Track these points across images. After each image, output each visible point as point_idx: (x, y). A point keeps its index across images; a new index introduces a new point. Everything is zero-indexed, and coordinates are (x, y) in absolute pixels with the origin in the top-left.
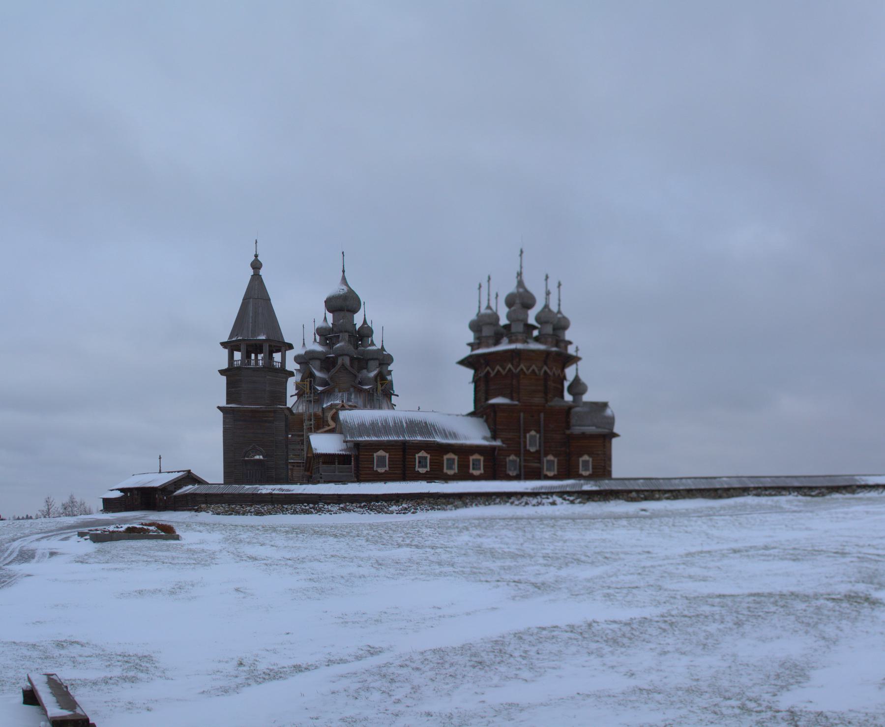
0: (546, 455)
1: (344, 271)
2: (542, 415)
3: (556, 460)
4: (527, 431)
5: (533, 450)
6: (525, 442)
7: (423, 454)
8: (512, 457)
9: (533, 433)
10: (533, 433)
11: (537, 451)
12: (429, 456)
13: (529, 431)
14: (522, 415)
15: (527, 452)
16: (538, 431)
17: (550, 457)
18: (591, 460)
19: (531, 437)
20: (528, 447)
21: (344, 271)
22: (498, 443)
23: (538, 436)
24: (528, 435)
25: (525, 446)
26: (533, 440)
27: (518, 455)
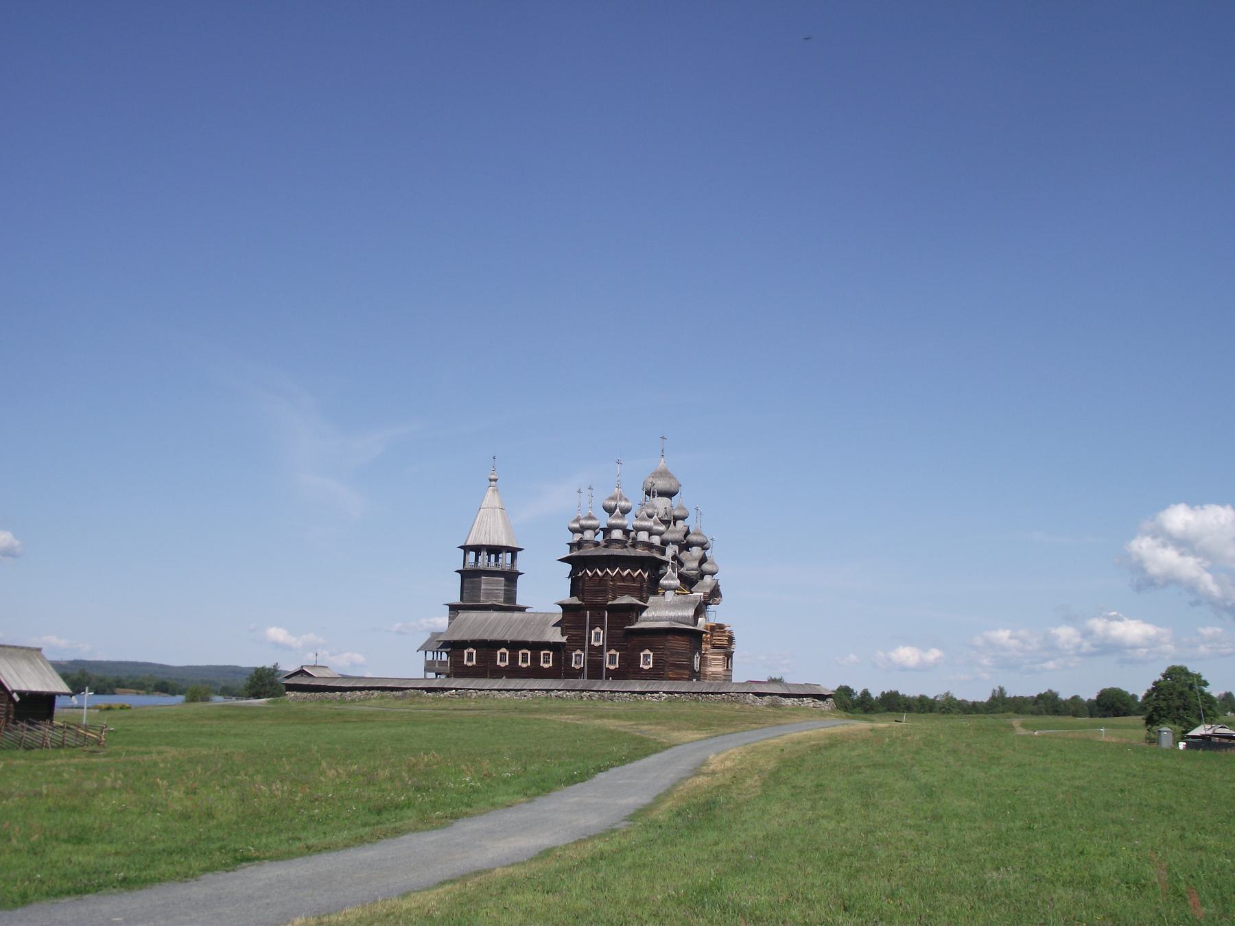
4: (591, 628)
5: (597, 644)
8: (578, 652)
9: (598, 629)
10: (598, 629)
15: (591, 647)
16: (602, 628)
17: (613, 652)
22: (564, 640)
27: (583, 650)
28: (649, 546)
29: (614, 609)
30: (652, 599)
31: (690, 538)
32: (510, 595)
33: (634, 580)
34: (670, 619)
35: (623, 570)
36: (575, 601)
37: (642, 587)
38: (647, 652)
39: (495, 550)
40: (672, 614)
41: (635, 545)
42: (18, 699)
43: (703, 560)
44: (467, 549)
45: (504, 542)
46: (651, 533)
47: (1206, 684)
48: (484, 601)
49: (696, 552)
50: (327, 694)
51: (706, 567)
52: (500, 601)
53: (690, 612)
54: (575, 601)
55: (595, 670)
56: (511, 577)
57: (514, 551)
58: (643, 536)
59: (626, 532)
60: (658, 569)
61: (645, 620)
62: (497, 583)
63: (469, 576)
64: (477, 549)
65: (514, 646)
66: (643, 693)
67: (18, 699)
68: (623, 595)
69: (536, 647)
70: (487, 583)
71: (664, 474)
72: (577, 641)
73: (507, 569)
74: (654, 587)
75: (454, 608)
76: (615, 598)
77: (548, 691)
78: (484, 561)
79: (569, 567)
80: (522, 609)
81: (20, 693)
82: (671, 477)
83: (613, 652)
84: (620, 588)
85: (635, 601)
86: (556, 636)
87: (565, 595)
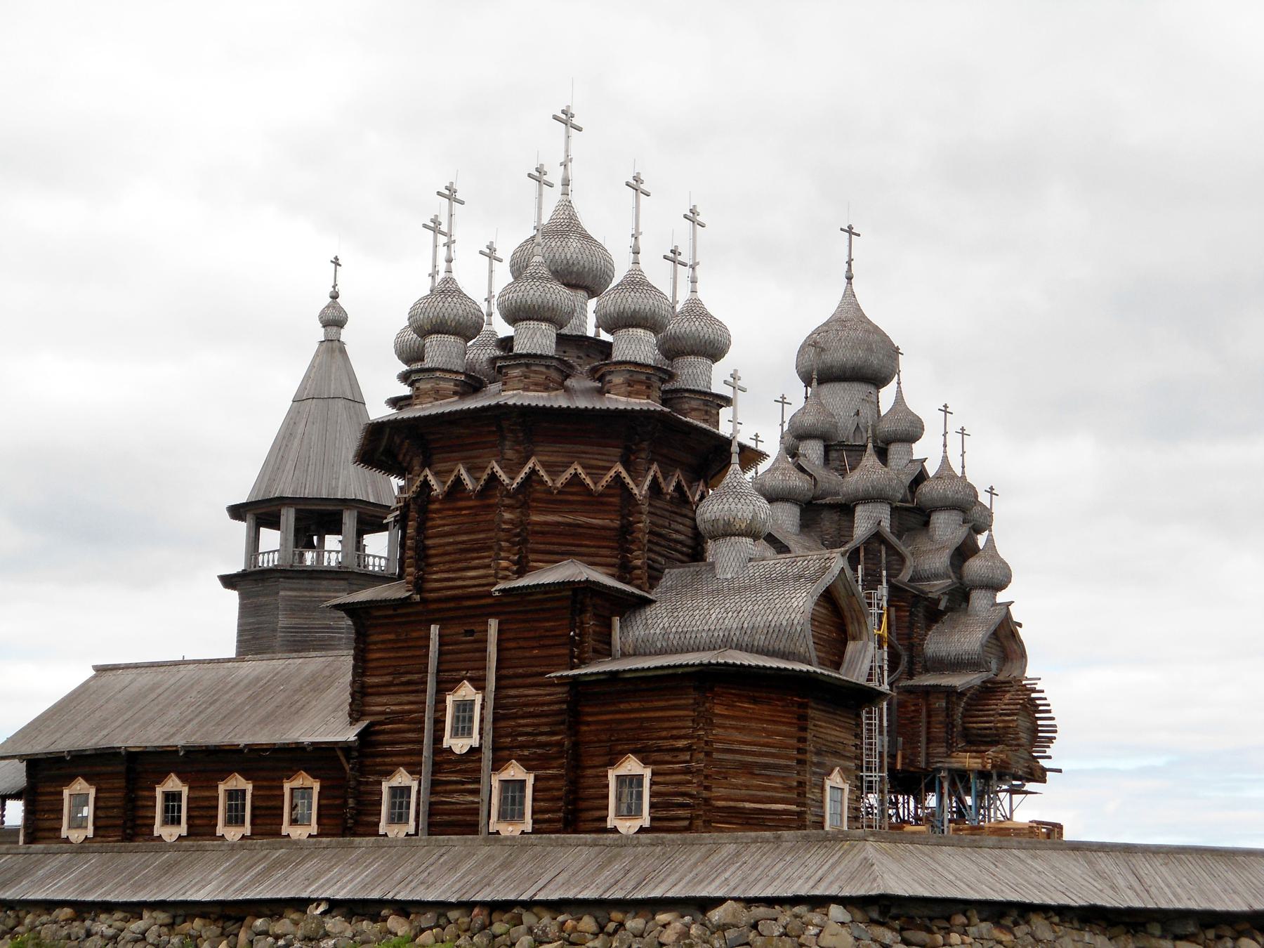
0: (498, 765)
1: (849, 278)
2: (493, 624)
3: (530, 779)
4: (446, 685)
5: (459, 745)
6: (439, 723)
7: (173, 783)
9: (466, 691)
10: (466, 691)
11: (472, 750)
12: (185, 791)
13: (453, 684)
14: (434, 630)
15: (442, 756)
16: (479, 684)
17: (515, 771)
18: (647, 773)
19: (464, 707)
20: (447, 741)
21: (849, 278)
23: (478, 698)
24: (450, 699)
25: (438, 739)
26: (465, 717)
29: (523, 608)
31: (925, 488)
33: (593, 501)
35: (553, 470)
37: (626, 530)
38: (631, 765)
51: (975, 566)
65: (205, 764)
68: (555, 557)
69: (270, 763)
76: (521, 573)
83: (515, 771)
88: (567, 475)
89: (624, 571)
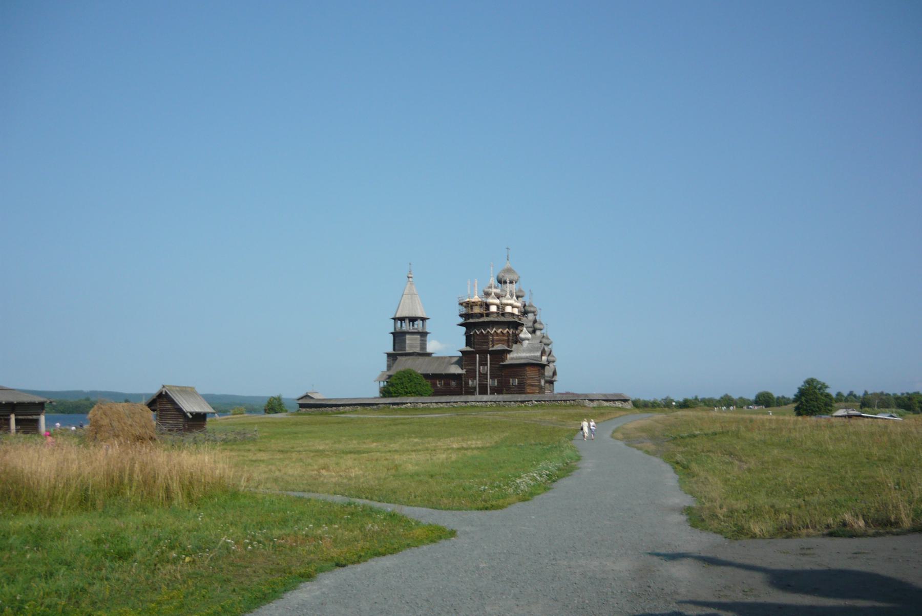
22: (464, 372)
28: (512, 314)
30: (515, 346)
32: (423, 345)
34: (527, 358)
36: (469, 349)
39: (413, 320)
40: (528, 355)
41: (503, 314)
42: (190, 416)
43: (535, 322)
44: (395, 319)
45: (420, 314)
46: (513, 307)
47: (827, 387)
48: (408, 350)
49: (531, 316)
50: (323, 409)
52: (418, 350)
53: (539, 354)
54: (469, 349)
55: (483, 391)
56: (424, 334)
57: (423, 319)
58: (508, 309)
59: (498, 308)
60: (517, 329)
61: (512, 359)
62: (416, 339)
63: (398, 336)
64: (402, 319)
66: (522, 402)
67: (190, 416)
70: (410, 340)
71: (509, 270)
72: (471, 374)
73: (420, 330)
74: (517, 340)
75: (389, 355)
77: (466, 402)
78: (406, 326)
79: (464, 329)
80: (429, 355)
81: (191, 413)
82: (514, 272)
84: (498, 340)
85: (505, 347)
86: (456, 370)
87: (463, 347)
88: (499, 331)
89: (508, 346)
